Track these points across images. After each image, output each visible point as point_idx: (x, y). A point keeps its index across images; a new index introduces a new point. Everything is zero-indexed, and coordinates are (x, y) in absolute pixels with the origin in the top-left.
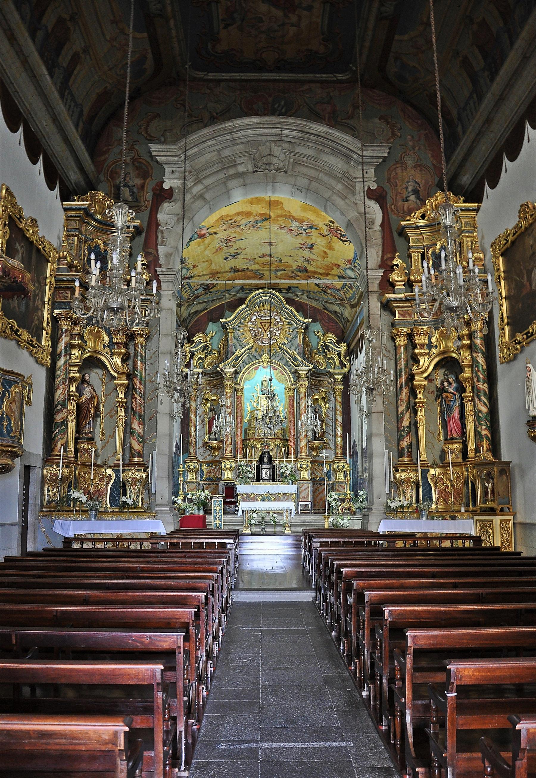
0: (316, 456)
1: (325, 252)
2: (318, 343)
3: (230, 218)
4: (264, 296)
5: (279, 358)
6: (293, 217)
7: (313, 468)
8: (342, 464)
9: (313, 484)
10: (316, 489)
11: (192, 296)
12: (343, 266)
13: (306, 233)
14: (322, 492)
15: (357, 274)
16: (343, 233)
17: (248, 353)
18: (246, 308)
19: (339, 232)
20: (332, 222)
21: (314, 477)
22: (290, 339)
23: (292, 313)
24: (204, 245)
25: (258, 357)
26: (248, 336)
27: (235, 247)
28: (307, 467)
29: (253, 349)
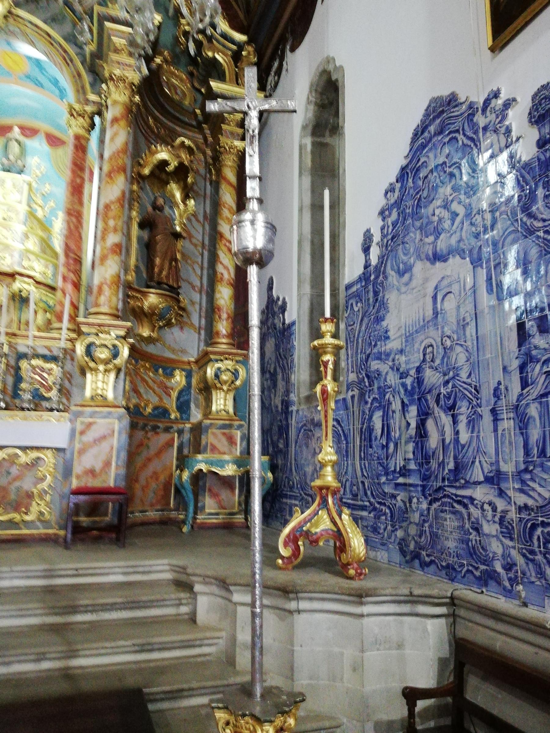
0: (150, 340)
7: (137, 374)
8: (229, 364)
9: (133, 426)
10: (141, 445)
14: (159, 453)
21: (137, 406)
28: (115, 355)
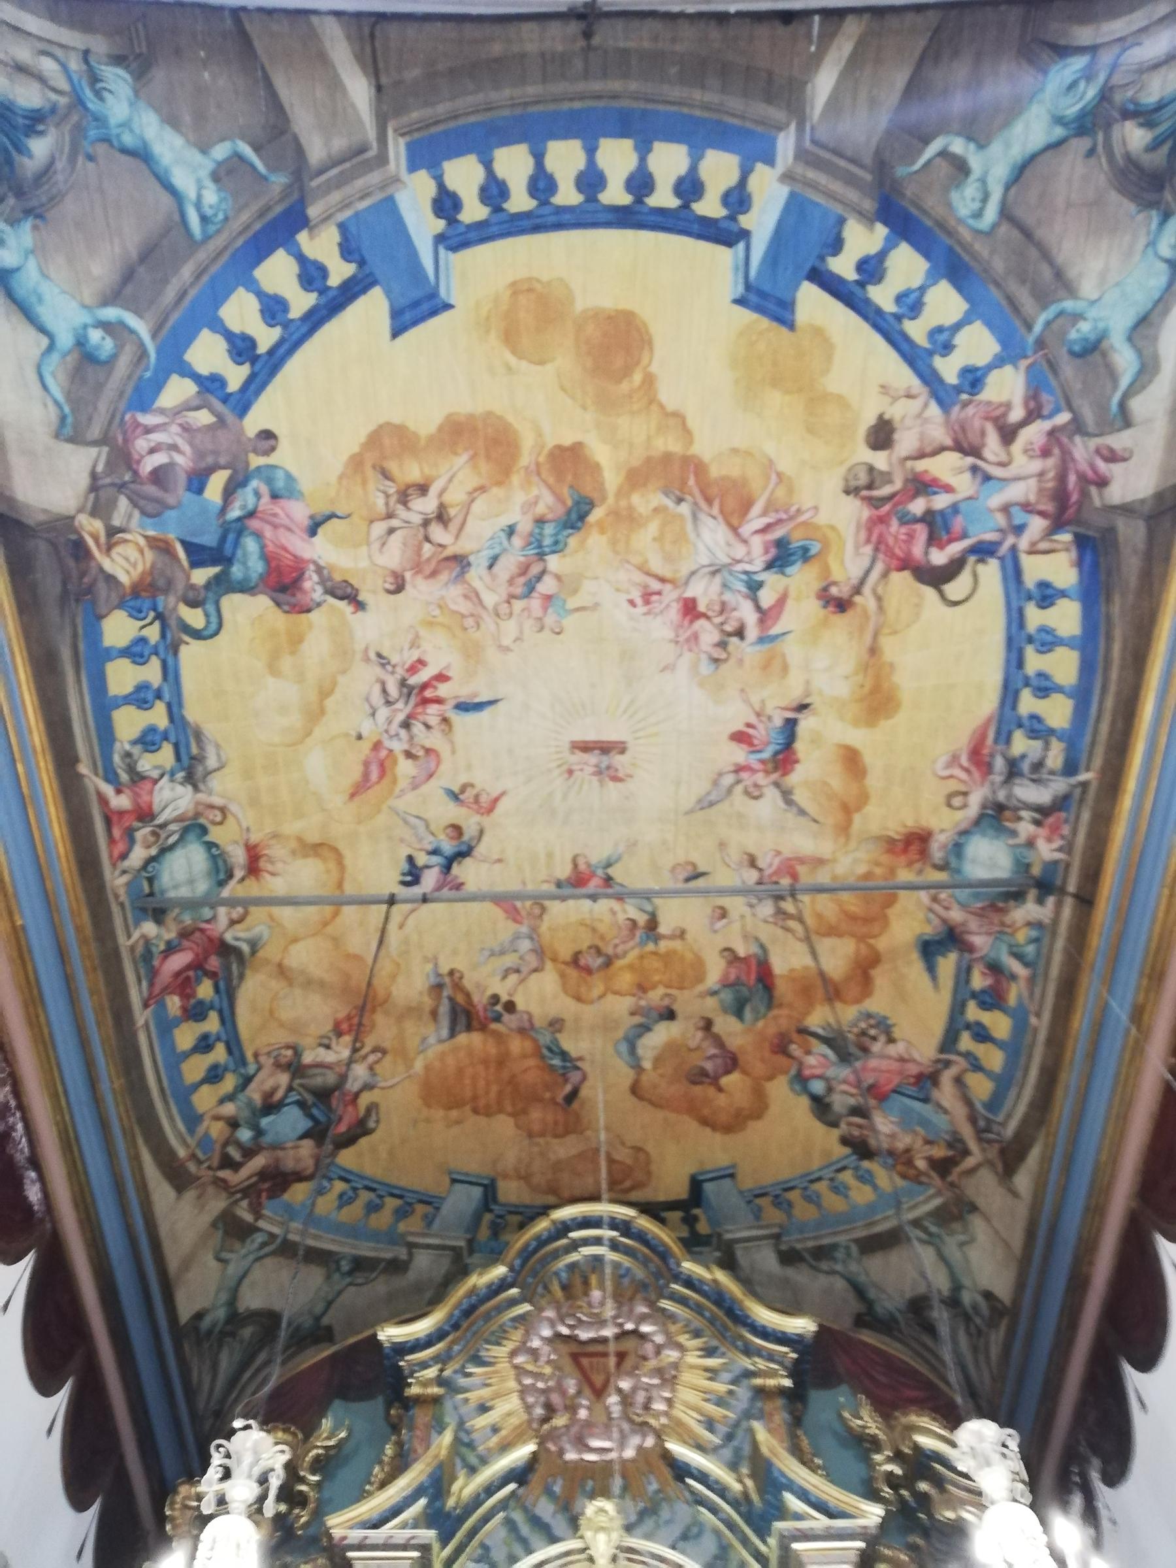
1: (852, 760)
2: (871, 1465)
3: (413, 472)
4: (586, 1242)
5: (677, 1530)
6: (698, 467)
11: (249, 1153)
12: (945, 825)
13: (766, 616)
15: (1025, 828)
16: (941, 502)
17: (503, 1505)
18: (502, 1285)
19: (918, 507)
20: (882, 435)
22: (723, 1429)
23: (719, 1298)
24: (300, 678)
25: (559, 1525)
26: (509, 1408)
27: (449, 776)
29: (535, 1479)
